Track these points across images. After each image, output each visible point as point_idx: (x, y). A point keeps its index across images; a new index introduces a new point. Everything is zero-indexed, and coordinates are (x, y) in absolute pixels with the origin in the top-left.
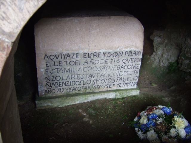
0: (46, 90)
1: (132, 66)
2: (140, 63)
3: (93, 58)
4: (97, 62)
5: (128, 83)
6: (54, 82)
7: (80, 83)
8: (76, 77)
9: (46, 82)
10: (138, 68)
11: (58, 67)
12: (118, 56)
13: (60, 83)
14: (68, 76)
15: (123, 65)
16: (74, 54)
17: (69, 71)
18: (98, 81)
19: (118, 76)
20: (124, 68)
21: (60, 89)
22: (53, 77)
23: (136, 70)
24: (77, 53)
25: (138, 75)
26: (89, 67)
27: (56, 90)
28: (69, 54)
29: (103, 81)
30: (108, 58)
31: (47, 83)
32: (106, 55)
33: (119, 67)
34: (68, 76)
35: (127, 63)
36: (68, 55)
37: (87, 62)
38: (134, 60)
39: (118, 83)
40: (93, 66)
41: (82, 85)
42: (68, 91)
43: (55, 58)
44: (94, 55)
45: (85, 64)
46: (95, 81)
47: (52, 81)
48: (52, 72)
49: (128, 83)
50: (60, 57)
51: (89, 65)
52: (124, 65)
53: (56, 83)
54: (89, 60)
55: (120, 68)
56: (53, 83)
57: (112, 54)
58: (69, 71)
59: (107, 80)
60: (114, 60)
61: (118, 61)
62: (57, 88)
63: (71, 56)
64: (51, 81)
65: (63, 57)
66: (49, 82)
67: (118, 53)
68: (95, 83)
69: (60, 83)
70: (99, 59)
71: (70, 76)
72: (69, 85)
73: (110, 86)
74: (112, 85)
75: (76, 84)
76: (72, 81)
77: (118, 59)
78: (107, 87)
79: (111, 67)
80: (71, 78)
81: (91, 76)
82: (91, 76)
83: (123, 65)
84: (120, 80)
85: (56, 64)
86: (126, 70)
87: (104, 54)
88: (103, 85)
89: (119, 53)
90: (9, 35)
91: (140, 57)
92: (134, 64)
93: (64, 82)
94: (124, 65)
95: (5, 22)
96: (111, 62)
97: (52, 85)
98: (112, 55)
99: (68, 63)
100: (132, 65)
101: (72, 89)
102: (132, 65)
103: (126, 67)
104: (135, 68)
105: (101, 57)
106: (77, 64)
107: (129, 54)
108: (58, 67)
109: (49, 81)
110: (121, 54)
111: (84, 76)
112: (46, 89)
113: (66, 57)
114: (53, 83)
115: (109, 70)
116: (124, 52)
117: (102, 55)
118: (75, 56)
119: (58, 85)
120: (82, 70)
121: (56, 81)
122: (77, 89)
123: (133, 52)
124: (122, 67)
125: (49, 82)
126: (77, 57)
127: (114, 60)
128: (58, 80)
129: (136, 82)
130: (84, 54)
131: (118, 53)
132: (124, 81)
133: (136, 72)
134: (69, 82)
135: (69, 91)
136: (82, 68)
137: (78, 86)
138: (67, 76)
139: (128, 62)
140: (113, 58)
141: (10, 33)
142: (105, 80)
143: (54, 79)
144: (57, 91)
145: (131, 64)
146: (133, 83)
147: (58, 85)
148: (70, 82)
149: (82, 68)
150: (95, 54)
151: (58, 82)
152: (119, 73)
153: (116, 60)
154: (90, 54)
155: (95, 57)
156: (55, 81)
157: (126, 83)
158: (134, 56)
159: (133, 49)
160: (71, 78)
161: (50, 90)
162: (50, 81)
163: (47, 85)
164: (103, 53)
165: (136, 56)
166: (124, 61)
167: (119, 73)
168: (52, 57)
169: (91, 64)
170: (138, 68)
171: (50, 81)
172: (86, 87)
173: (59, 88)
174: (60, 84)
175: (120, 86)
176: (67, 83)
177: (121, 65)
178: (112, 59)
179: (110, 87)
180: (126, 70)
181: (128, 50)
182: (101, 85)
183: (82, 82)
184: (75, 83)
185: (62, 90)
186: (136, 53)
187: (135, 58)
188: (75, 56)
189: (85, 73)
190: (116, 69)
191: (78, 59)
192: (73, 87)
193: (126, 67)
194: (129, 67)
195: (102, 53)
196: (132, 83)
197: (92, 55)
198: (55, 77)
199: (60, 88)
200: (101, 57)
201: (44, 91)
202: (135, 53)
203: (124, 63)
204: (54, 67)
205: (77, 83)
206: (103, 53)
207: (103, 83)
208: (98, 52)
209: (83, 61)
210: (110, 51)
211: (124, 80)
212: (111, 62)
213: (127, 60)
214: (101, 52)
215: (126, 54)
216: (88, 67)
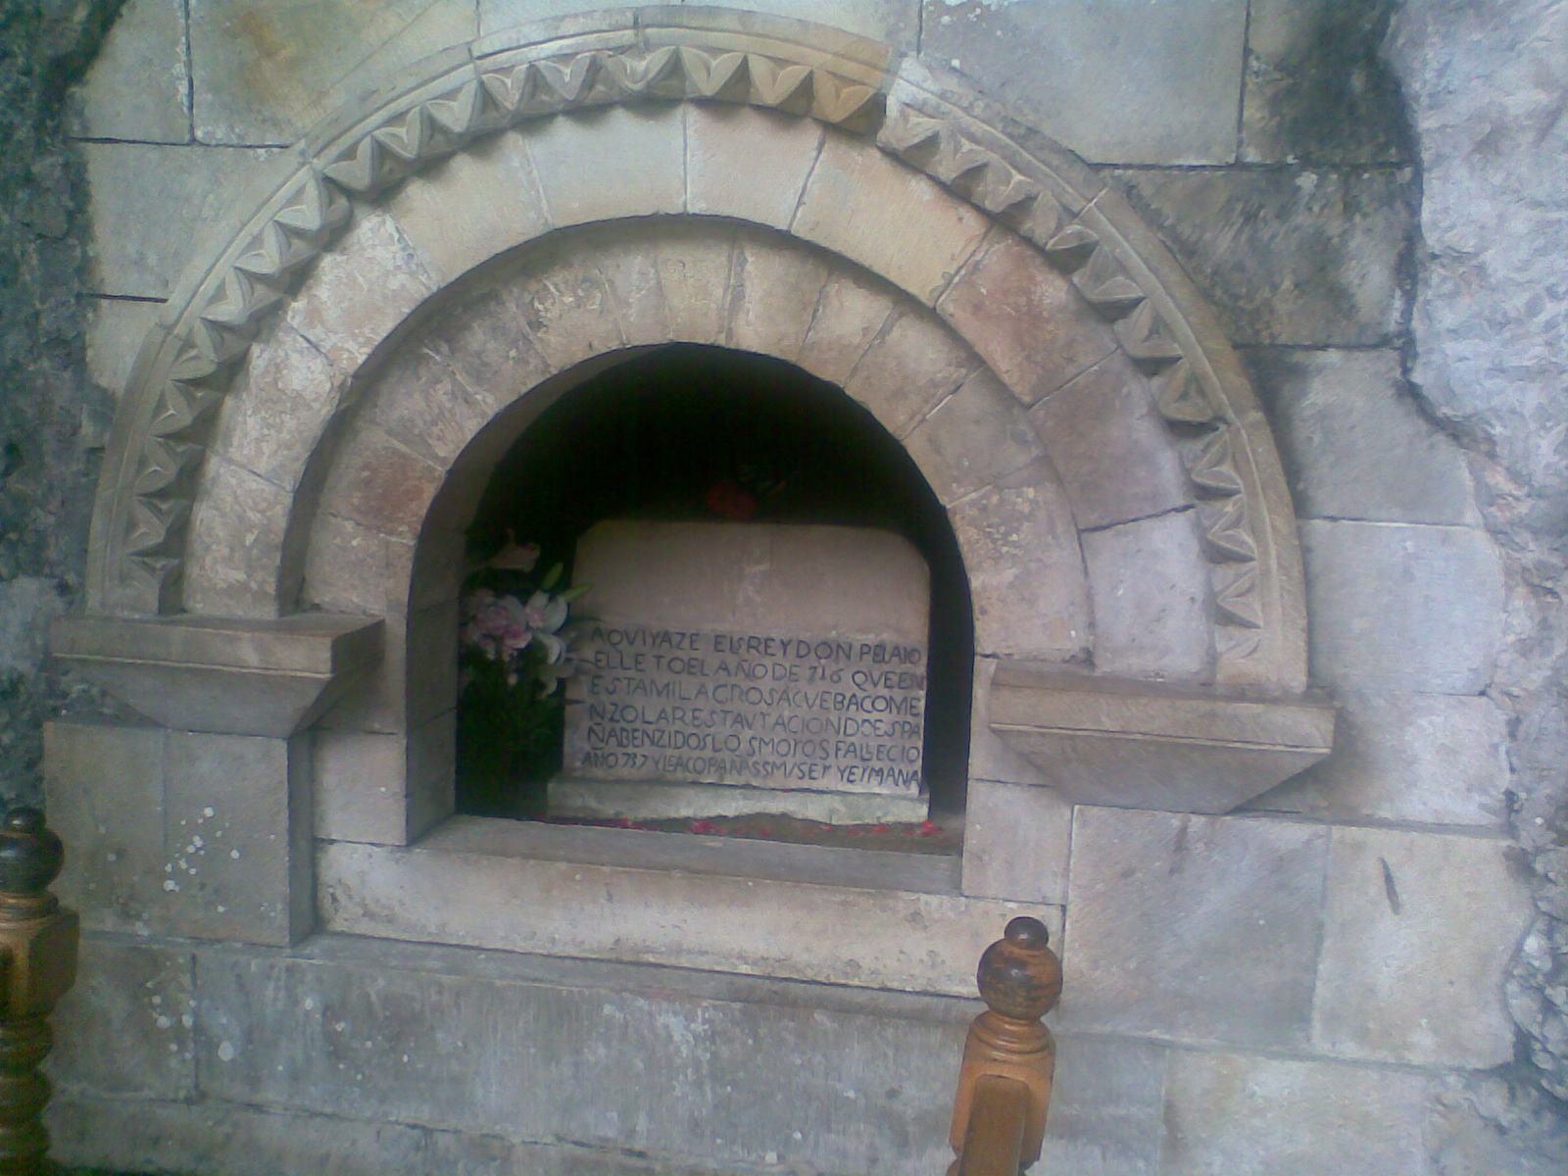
0: (588, 754)
1: (889, 701)
2: (922, 693)
3: (746, 657)
4: (760, 671)
5: (881, 770)
6: (618, 726)
7: (702, 743)
8: (689, 714)
9: (591, 723)
10: (914, 711)
11: (631, 673)
12: (833, 657)
13: (636, 734)
14: (663, 711)
15: (854, 695)
16: (683, 635)
17: (665, 692)
18: (767, 744)
19: (838, 733)
20: (860, 706)
21: (635, 755)
22: (613, 707)
23: (909, 718)
24: (694, 631)
25: (920, 744)
26: (734, 686)
27: (620, 756)
28: (666, 633)
29: (783, 748)
30: (798, 661)
31: (595, 727)
32: (792, 650)
33: (840, 698)
34: (663, 711)
35: (868, 686)
36: (666, 637)
37: (726, 669)
38: (895, 678)
39: (844, 762)
40: (745, 685)
41: (708, 753)
42: (660, 766)
43: (625, 642)
44: (750, 647)
45: (721, 672)
46: (756, 744)
47: (612, 719)
48: (611, 688)
49: (881, 770)
50: (639, 642)
51: (733, 680)
52: (860, 694)
53: (623, 729)
54: (732, 661)
55: (846, 702)
56: (613, 730)
57: (813, 647)
58: (665, 692)
59: (800, 746)
60: (820, 671)
61: (835, 678)
62: (625, 750)
63: (676, 639)
64: (606, 720)
65: (649, 640)
66: (599, 724)
67: (834, 647)
68: (757, 750)
69: (635, 730)
70: (768, 661)
71: (669, 710)
72: (663, 746)
73: (811, 771)
74: (819, 768)
75: (689, 745)
76: (677, 732)
77: (834, 668)
78: (801, 775)
79: (811, 696)
80: (671, 719)
81: (741, 722)
82: (739, 719)
83: (854, 695)
84: (848, 751)
85: (628, 661)
86: (866, 716)
87: (784, 645)
88: (784, 764)
89: (839, 646)
90: (443, 461)
91: (921, 669)
92: (898, 695)
93: (650, 728)
94: (860, 694)
95: (441, 443)
96: (811, 679)
97: (610, 736)
98: (813, 654)
99: (665, 662)
100: (891, 698)
101: (674, 761)
102: (891, 698)
103: (867, 704)
104: (903, 711)
105: (773, 655)
106: (693, 670)
107: (875, 654)
108: (631, 673)
109: (598, 720)
110: (847, 652)
111: (715, 716)
112: (587, 748)
113: (658, 641)
114: (613, 730)
115: (805, 705)
116: (857, 647)
117: (775, 648)
118: (686, 643)
119: (627, 738)
120: (710, 694)
121: (623, 724)
122: (691, 765)
123: (889, 649)
124: (854, 700)
125: (599, 724)
126: (695, 646)
127: (820, 671)
128: (631, 722)
129: (916, 773)
130: (718, 639)
131: (834, 647)
132: (863, 759)
133: (907, 727)
134: (663, 732)
135: (664, 769)
136: (710, 688)
137: (696, 754)
138: (659, 709)
139: (875, 685)
140: (816, 664)
141: (445, 458)
142: (792, 744)
143: (617, 717)
144: (622, 760)
145: (886, 692)
146: (900, 772)
147: (627, 738)
148: (667, 733)
149: (710, 688)
150: (754, 643)
151: (629, 727)
152: (843, 723)
153: (828, 673)
154: (735, 639)
155: (753, 651)
156: (618, 721)
157: (873, 769)
158: (896, 666)
159: (888, 637)
160: (671, 719)
161: (599, 752)
162: (603, 718)
163: (592, 735)
164: (782, 642)
165: (903, 666)
166: (860, 678)
167: (843, 723)
168: (616, 638)
169: (741, 675)
170: (914, 711)
171: (603, 718)
172: (723, 761)
173: (630, 750)
174: (635, 738)
175: (851, 778)
176: (657, 735)
177: (848, 695)
178: (815, 668)
179: (814, 774)
180: (866, 716)
181: (871, 639)
182: (778, 762)
183: (709, 740)
184: (686, 742)
185: (639, 760)
186: (902, 651)
187: (898, 671)
188: (686, 643)
189: (719, 707)
190: (830, 704)
191: (694, 654)
192: (676, 753)
193: (867, 704)
194: (881, 704)
195: (778, 642)
196: (897, 772)
197: (744, 647)
198: (620, 707)
199: (636, 750)
200: (773, 655)
201: (581, 756)
202: (899, 655)
203: (858, 685)
204: (621, 673)
205: (693, 742)
206: (782, 642)
207: (786, 755)
208: (761, 634)
209: (713, 661)
210: (805, 636)
211: (867, 756)
212: (811, 679)
213: (868, 676)
214: (773, 636)
215: (862, 653)
216: (729, 687)
